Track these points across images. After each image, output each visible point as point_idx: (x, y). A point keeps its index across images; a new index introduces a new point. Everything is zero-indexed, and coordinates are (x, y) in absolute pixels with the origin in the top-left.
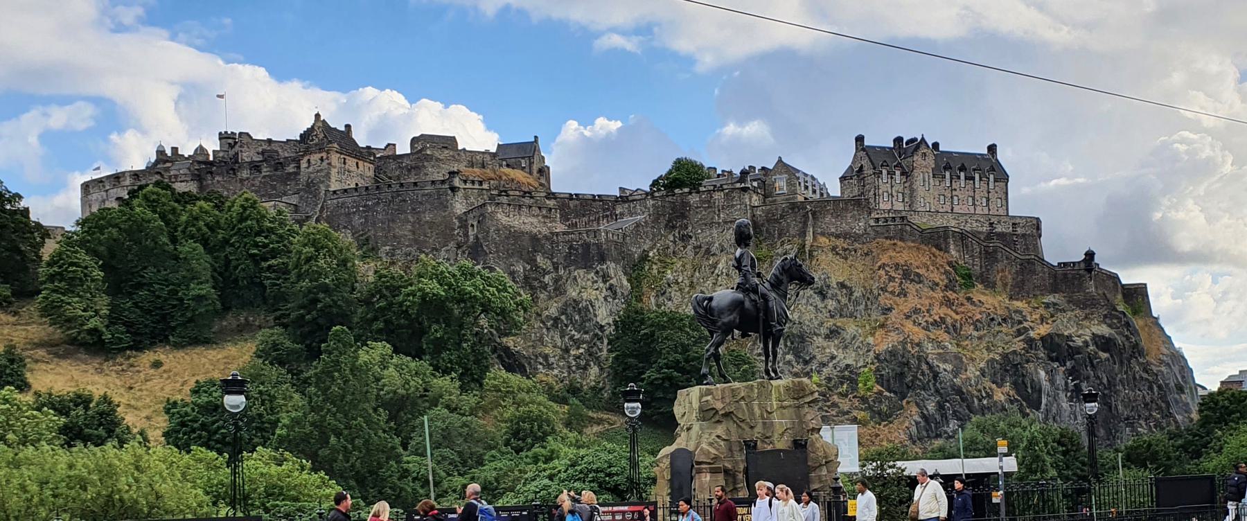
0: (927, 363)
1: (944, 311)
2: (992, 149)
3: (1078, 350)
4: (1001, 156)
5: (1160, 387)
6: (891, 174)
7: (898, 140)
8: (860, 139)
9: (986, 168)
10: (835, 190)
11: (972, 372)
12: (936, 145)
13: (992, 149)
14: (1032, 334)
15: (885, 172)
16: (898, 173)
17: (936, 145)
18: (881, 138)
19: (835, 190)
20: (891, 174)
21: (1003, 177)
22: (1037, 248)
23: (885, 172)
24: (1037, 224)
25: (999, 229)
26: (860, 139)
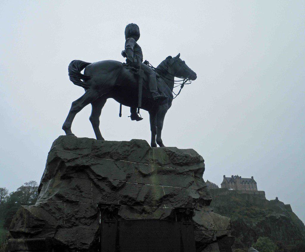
0: (244, 223)
1: (246, 211)
2: (252, 177)
3: (277, 220)
4: (254, 179)
5: (297, 228)
6: (232, 183)
7: (232, 176)
8: (224, 176)
9: (252, 181)
10: (220, 187)
11: (254, 225)
12: (240, 177)
13: (252, 177)
14: (267, 216)
15: (230, 182)
16: (233, 183)
17: (240, 177)
18: (229, 176)
19: (220, 187)
20: (232, 183)
21: (256, 183)
22: (265, 197)
23: (230, 182)
24: (264, 192)
25: (256, 193)
26: (224, 176)
